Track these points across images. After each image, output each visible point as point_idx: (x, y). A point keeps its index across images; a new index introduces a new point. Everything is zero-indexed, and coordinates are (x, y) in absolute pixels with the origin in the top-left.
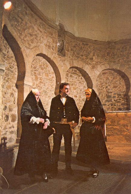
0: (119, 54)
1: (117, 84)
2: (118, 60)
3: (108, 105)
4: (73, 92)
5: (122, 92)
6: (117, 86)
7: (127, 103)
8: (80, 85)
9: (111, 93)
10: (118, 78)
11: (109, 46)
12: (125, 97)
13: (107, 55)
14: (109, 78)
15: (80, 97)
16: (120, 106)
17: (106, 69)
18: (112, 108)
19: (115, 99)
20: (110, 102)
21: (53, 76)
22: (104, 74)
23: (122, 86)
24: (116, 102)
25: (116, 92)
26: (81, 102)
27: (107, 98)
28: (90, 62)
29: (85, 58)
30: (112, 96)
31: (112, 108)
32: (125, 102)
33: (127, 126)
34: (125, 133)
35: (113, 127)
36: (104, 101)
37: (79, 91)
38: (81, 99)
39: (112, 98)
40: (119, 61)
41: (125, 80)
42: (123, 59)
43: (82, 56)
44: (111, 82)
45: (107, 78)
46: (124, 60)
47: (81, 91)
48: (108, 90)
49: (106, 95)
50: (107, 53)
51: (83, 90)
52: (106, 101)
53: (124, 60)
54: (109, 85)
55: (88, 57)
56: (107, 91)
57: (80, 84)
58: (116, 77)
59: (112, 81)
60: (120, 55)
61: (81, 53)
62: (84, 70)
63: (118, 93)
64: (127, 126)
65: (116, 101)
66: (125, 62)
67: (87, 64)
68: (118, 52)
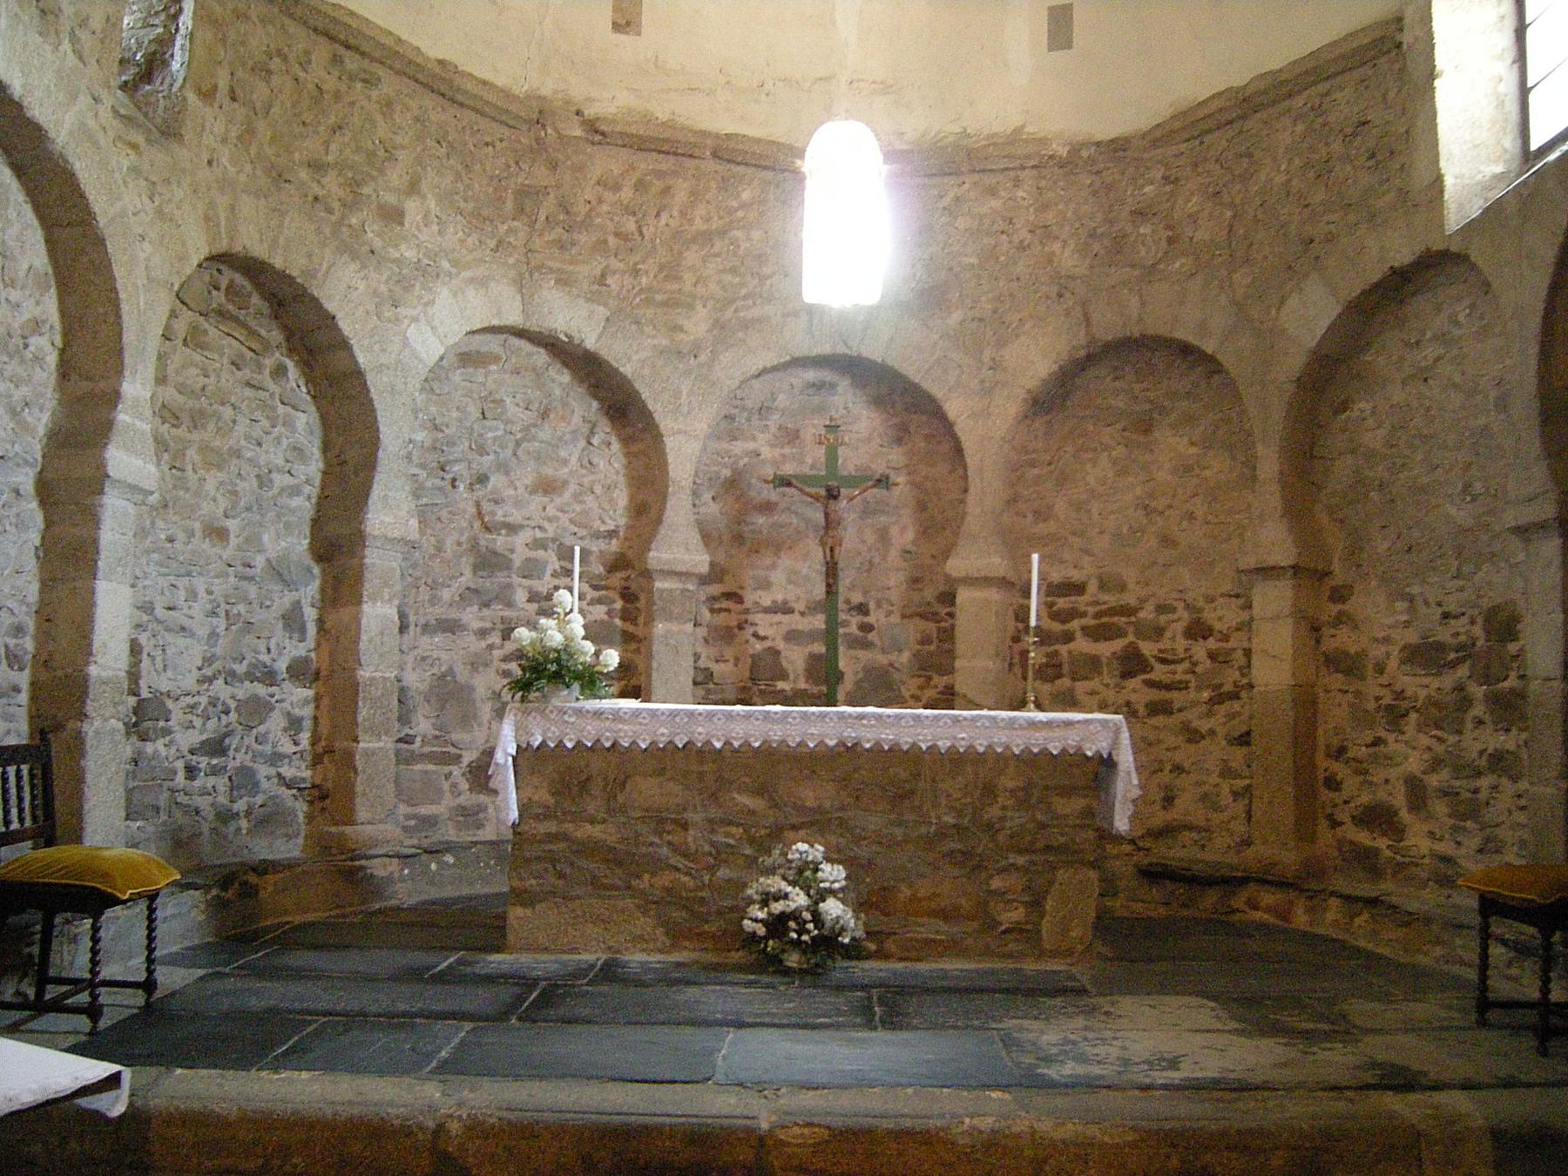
0: (610, 226)
1: (565, 462)
2: (598, 272)
3: (483, 633)
4: (197, 494)
5: (597, 535)
6: (565, 483)
7: (631, 629)
8: (257, 432)
9: (512, 529)
10: (576, 419)
12: (623, 574)
13: (520, 210)
14: (508, 401)
15: (253, 541)
17: (495, 322)
18: (505, 659)
20: (498, 610)
21: (37, 312)
22: (468, 359)
23: (598, 490)
25: (551, 530)
26: (253, 591)
27: (476, 568)
28: (378, 244)
29: (341, 193)
30: (517, 561)
31: (505, 659)
32: (609, 613)
33: (685, 826)
34: (665, 879)
35: (569, 827)
36: (446, 594)
37: (248, 486)
38: (259, 561)
39: (516, 580)
40: (602, 279)
41: (626, 441)
42: (636, 273)
43: (317, 167)
44: (518, 444)
47: (263, 481)
48: (487, 507)
49: (474, 546)
50: (523, 193)
51: (280, 480)
54: (503, 468)
55: (366, 190)
57: (265, 423)
58: (565, 405)
59: (526, 429)
60: (617, 235)
61: (311, 146)
62: (315, 302)
64: (685, 826)
66: (648, 302)
67: (355, 256)
68: (605, 208)
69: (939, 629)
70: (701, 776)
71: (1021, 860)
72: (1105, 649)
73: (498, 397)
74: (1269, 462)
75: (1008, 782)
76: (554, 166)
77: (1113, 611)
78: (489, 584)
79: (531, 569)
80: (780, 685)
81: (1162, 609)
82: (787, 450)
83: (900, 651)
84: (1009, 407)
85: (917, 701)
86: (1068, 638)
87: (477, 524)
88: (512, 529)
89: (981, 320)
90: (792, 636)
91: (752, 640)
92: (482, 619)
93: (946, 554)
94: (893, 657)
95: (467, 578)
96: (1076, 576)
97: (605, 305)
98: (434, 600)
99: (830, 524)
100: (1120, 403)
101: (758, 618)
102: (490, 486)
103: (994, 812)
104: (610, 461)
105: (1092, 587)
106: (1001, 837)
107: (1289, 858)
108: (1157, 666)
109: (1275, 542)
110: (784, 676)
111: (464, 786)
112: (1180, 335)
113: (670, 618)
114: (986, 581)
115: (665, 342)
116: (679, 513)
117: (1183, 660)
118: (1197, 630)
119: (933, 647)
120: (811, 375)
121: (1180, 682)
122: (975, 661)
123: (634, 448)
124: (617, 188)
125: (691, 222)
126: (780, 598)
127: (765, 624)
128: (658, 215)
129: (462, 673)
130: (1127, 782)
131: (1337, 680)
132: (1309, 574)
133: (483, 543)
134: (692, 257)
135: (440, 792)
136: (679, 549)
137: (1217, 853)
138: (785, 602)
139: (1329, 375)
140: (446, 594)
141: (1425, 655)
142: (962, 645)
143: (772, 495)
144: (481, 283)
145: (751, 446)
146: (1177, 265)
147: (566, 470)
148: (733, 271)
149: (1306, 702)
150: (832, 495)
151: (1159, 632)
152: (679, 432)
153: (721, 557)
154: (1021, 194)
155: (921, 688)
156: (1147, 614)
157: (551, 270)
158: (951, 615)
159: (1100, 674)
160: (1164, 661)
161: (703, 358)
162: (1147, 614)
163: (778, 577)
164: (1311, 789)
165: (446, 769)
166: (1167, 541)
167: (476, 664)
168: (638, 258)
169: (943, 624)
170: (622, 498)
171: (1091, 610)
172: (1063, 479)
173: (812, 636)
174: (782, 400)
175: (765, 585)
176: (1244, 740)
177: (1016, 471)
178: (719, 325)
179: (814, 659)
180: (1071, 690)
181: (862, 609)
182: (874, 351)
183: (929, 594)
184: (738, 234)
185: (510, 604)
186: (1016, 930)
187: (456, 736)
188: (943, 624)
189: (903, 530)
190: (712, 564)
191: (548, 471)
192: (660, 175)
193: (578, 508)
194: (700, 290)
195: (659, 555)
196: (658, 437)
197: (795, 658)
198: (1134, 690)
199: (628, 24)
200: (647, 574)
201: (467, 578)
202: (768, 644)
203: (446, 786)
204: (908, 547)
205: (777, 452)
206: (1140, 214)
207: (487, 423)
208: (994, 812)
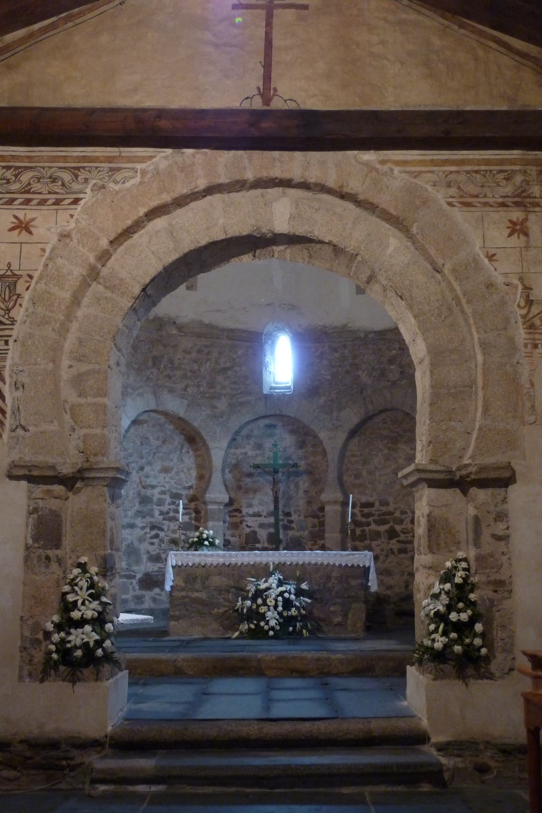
3: (143, 528)
5: (185, 488)
6: (172, 468)
9: (153, 487)
10: (176, 443)
11: (161, 336)
12: (196, 503)
13: (154, 364)
14: (150, 438)
16: (174, 532)
17: (147, 409)
18: (152, 538)
19: (162, 508)
20: (148, 519)
22: (135, 422)
23: (185, 470)
24: (164, 519)
25: (167, 486)
27: (140, 503)
30: (155, 499)
31: (152, 538)
32: (190, 519)
35: (190, 593)
36: (130, 514)
39: (155, 507)
40: (185, 389)
42: (198, 386)
44: (154, 454)
45: (145, 440)
46: (202, 389)
48: (143, 479)
49: (139, 494)
50: (154, 358)
52: (140, 514)
53: (202, 389)
54: (150, 463)
56: (141, 482)
59: (157, 448)
60: (191, 371)
63: (174, 491)
65: (166, 516)
68: (186, 361)
69: (319, 522)
70: (233, 575)
71: (340, 601)
72: (382, 528)
73: (147, 436)
75: (335, 574)
76: (165, 346)
77: (384, 514)
78: (146, 509)
79: (160, 503)
80: (257, 545)
81: (403, 512)
82: (258, 452)
83: (304, 531)
86: (368, 524)
87: (140, 486)
88: (153, 487)
89: (332, 401)
90: (262, 526)
91: (246, 528)
92: (143, 522)
93: (321, 491)
94: (301, 533)
95: (137, 507)
96: (371, 500)
97: (187, 399)
98: (126, 516)
101: (247, 519)
102: (145, 471)
103: (330, 585)
104: (189, 460)
105: (377, 504)
106: (333, 593)
108: (402, 535)
110: (259, 542)
111: (137, 587)
113: (213, 519)
114: (335, 502)
115: (210, 413)
116: (217, 479)
117: (410, 532)
119: (317, 529)
120: (267, 421)
121: (410, 540)
122: (332, 535)
123: (199, 453)
124: (189, 353)
125: (219, 364)
126: (256, 510)
127: (250, 521)
128: (206, 363)
129: (136, 544)
133: (142, 493)
134: (220, 378)
135: (128, 589)
136: (217, 494)
138: (258, 512)
140: (130, 514)
142: (327, 527)
143: (253, 470)
144: (141, 395)
145: (244, 451)
146: (403, 382)
147: (172, 463)
148: (235, 383)
151: (401, 522)
152: (216, 447)
153: (233, 495)
154: (346, 351)
155: (313, 545)
156: (397, 514)
157: (166, 387)
158: (324, 516)
159: (381, 538)
160: (404, 533)
161: (224, 418)
162: (397, 514)
163: (255, 502)
165: (130, 581)
167: (141, 540)
168: (198, 380)
169: (321, 520)
170: (194, 473)
171: (377, 513)
172: (365, 462)
173: (269, 525)
174: (256, 432)
175: (250, 506)
178: (230, 405)
179: (270, 535)
180: (370, 544)
182: (291, 412)
183: (315, 507)
184: (237, 368)
185: (152, 516)
186: (339, 624)
187: (135, 568)
188: (321, 520)
189: (304, 483)
190: (230, 498)
191: (166, 464)
192: (206, 346)
193: (177, 478)
194: (223, 392)
195: (210, 496)
196: (207, 449)
197: (263, 534)
198: (393, 544)
199: (192, 286)
200: (205, 503)
201: (137, 507)
202: (252, 529)
203: (131, 587)
204: (307, 489)
205: (254, 453)
206: (391, 361)
207: (144, 447)
208: (330, 585)
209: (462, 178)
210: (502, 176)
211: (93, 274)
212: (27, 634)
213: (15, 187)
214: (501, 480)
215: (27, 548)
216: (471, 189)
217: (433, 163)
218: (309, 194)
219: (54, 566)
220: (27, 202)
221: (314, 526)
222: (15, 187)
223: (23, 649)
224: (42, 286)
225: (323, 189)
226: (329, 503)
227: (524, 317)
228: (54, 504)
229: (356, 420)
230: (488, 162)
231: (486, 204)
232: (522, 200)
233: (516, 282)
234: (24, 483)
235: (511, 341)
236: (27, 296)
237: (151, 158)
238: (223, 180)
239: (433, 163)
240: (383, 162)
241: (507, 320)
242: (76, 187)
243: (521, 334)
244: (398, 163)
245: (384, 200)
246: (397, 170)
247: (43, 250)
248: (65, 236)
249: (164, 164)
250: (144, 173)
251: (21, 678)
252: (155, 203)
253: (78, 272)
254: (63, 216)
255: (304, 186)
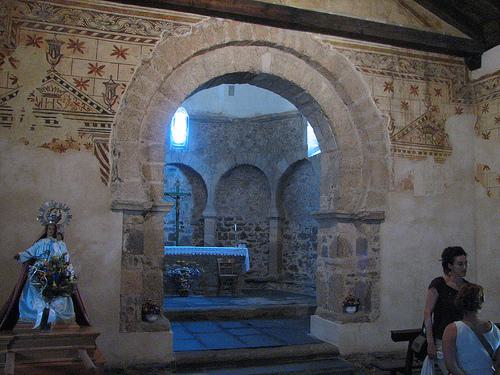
74: (273, 197)
84: (217, 178)
85: (194, 244)
90: (166, 229)
93: (202, 211)
99: (177, 204)
100: (242, 178)
107: (276, 276)
109: (274, 212)
112: (256, 165)
114: (211, 217)
118: (257, 229)
120: (170, 167)
122: (209, 236)
130: (247, 262)
131: (285, 240)
132: (281, 219)
137: (262, 277)
139: (287, 178)
141: (303, 236)
149: (280, 246)
150: (178, 198)
151: (250, 229)
164: (281, 263)
166: (251, 209)
176: (268, 253)
177: (218, 191)
181: (182, 223)
182: (186, 163)
209: (363, 55)
210: (381, 58)
211: (159, 89)
212: (124, 304)
213: (116, 28)
214: (377, 219)
215: (123, 253)
216: (367, 62)
217: (350, 46)
218: (281, 52)
219: (140, 265)
220: (123, 38)
221: (196, 230)
222: (116, 28)
223: (122, 313)
224: (131, 92)
225: (291, 51)
226: (208, 217)
227: (391, 134)
228: (139, 227)
229: (226, 170)
230: (376, 49)
231: (374, 72)
232: (390, 72)
233: (387, 115)
234: (121, 214)
235: (384, 147)
236: (122, 97)
237: (199, 20)
238: (240, 39)
239: (350, 46)
240: (325, 41)
241: (383, 136)
242: (153, 32)
243: (389, 144)
244: (332, 43)
245: (325, 62)
246: (332, 46)
247: (133, 69)
248: (146, 62)
249: (206, 26)
250: (194, 29)
251: (121, 330)
252: (200, 48)
253: (154, 85)
254: (146, 50)
255: (281, 48)
